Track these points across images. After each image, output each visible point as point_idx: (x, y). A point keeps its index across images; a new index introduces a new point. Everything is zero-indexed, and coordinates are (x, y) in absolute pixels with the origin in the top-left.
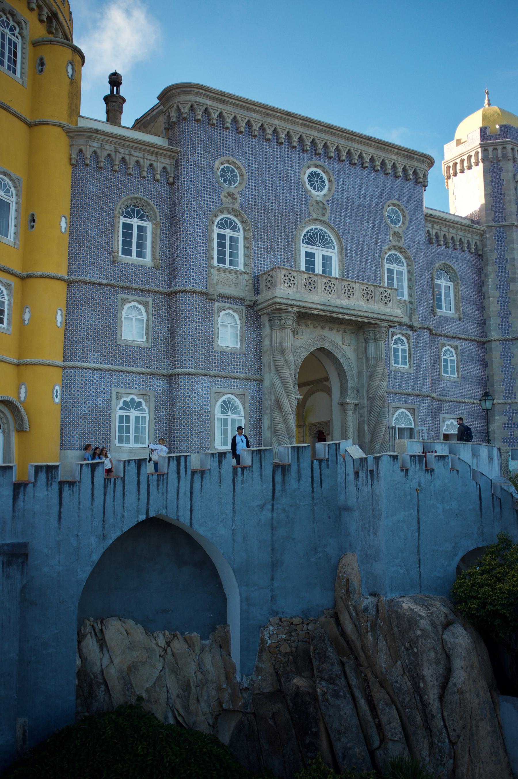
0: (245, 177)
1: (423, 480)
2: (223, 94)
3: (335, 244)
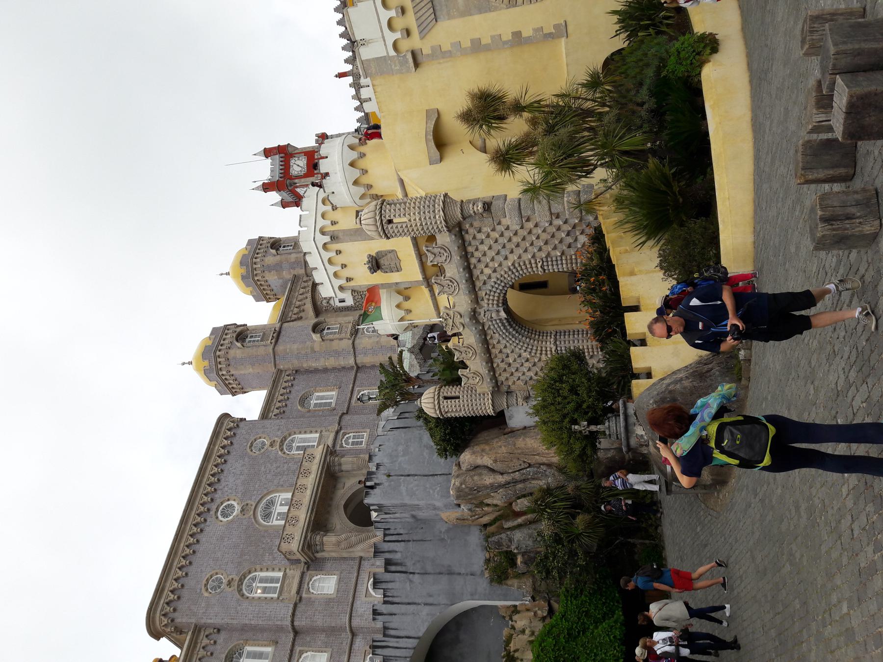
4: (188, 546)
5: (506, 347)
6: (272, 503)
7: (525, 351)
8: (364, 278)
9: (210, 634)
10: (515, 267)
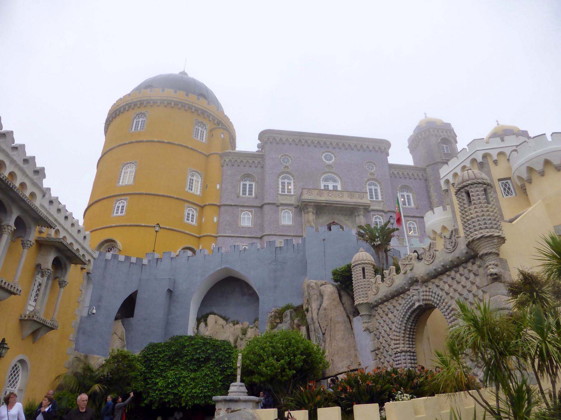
3: (339, 180)
4: (306, 141)
5: (398, 310)
6: (335, 181)
10: (451, 311)
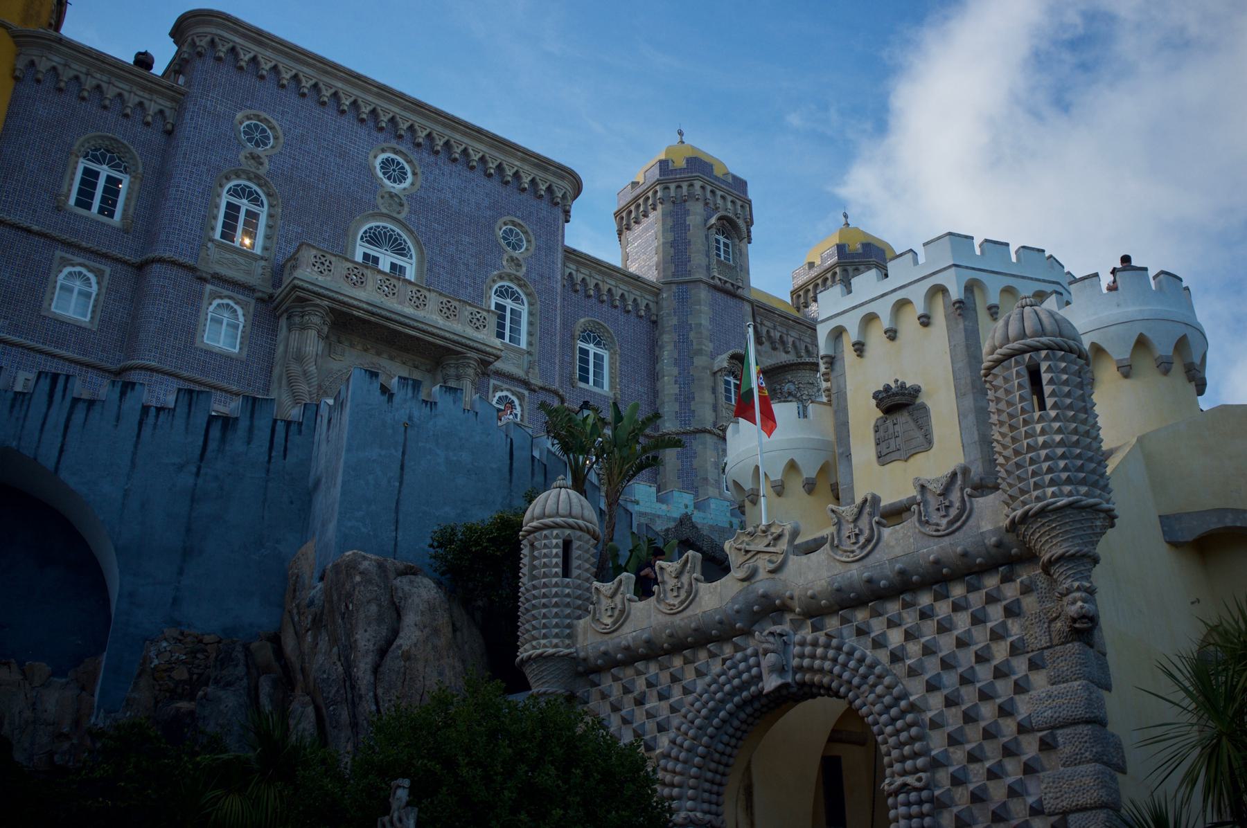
0: (281, 140)
1: (416, 413)
2: (259, 32)
4: (335, 94)
6: (401, 250)
7: (673, 742)
8: (862, 381)
9: (164, 118)
10: (903, 713)
